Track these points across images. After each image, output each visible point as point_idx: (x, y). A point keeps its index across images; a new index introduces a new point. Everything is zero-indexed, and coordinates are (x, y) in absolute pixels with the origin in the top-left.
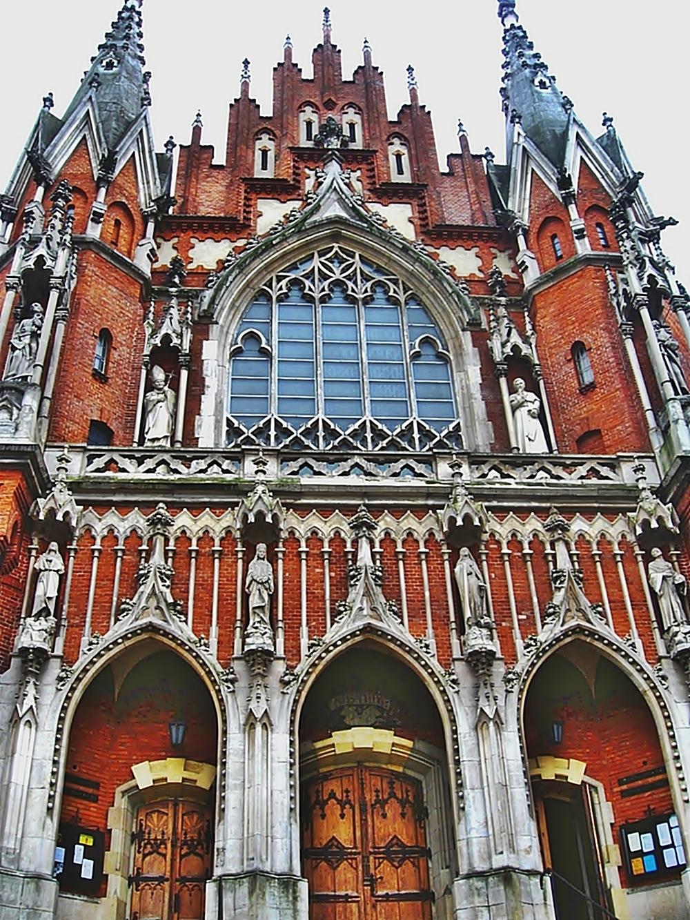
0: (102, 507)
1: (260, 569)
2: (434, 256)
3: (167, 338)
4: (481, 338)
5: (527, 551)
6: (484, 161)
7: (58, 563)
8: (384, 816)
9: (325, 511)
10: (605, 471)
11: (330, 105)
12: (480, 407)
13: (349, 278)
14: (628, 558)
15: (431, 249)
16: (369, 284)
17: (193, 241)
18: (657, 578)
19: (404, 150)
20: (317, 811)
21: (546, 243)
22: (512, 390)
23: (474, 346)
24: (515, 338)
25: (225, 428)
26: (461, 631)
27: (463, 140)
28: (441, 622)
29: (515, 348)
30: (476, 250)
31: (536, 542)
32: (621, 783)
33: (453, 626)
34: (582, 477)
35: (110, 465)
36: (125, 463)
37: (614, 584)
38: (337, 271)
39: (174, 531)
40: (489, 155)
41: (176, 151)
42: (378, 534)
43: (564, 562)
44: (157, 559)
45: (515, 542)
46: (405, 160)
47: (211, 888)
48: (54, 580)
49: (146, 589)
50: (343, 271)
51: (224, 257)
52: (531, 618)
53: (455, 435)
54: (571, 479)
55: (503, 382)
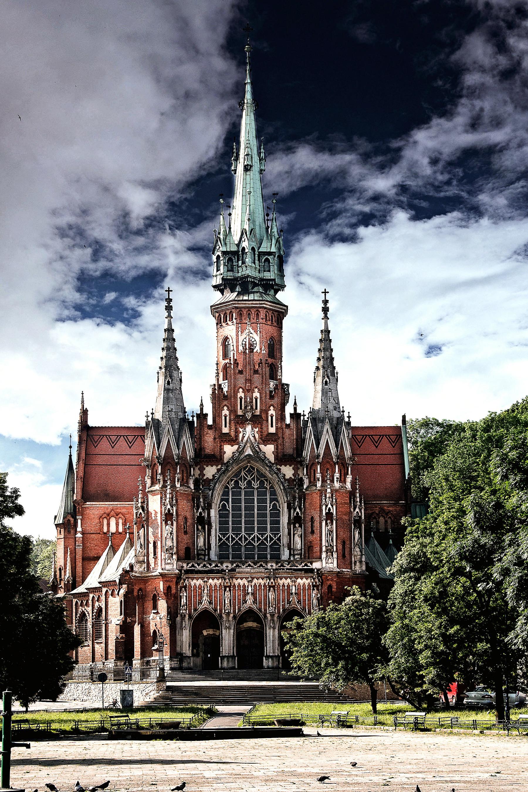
0: (193, 579)
1: (227, 594)
2: (279, 470)
3: (201, 513)
4: (289, 508)
5: (286, 588)
6: (302, 418)
7: (185, 594)
9: (242, 579)
10: (309, 564)
11: (248, 391)
12: (286, 530)
13: (253, 479)
14: (309, 589)
15: (279, 467)
16: (258, 482)
17: (205, 466)
18: (314, 595)
21: (312, 471)
22: (295, 527)
24: (298, 510)
25: (218, 538)
26: (269, 607)
27: (295, 409)
28: (265, 605)
29: (298, 513)
30: (293, 466)
31: (288, 586)
35: (193, 566)
36: (196, 565)
37: (304, 595)
39: (208, 584)
40: (304, 415)
41: (195, 419)
42: (253, 584)
43: (294, 591)
44: (206, 591)
45: (284, 585)
46: (274, 418)
48: (185, 597)
49: (204, 599)
52: (285, 604)
53: (279, 539)
54: (300, 567)
55: (292, 526)
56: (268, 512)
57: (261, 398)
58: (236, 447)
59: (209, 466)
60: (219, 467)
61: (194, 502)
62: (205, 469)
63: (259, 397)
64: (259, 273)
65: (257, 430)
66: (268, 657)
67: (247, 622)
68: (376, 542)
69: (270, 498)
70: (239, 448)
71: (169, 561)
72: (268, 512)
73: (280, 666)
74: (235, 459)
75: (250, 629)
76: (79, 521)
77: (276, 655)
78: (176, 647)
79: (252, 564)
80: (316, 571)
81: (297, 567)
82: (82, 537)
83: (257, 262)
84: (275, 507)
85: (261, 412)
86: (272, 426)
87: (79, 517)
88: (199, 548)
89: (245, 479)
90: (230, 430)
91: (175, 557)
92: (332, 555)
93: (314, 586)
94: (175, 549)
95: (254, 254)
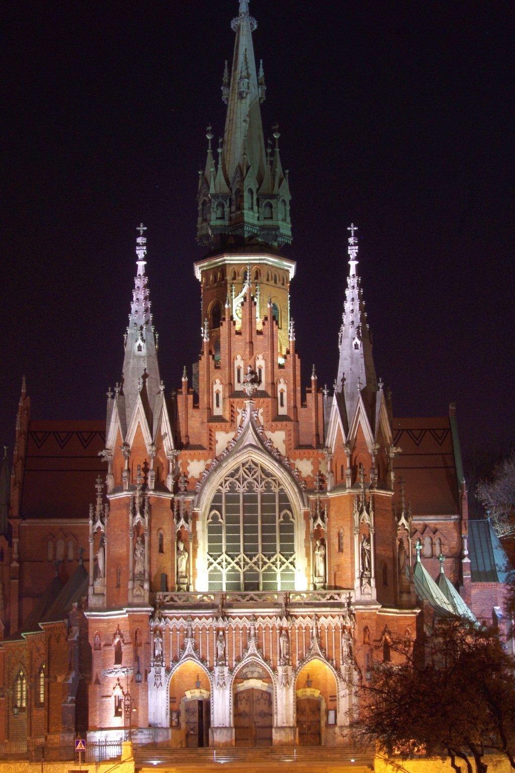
8: (259, 704)
16: (263, 483)
18: (343, 640)
19: (285, 389)
20: (239, 703)
23: (305, 518)
24: (319, 521)
29: (319, 526)
32: (330, 697)
33: (278, 655)
34: (328, 600)
38: (250, 475)
46: (285, 395)
47: (210, 731)
50: (253, 475)
51: (202, 471)
54: (324, 601)
56: (277, 524)
57: (267, 367)
58: (232, 435)
59: (195, 461)
60: (209, 461)
61: (173, 511)
62: (189, 464)
63: (264, 366)
64: (258, 219)
65: (261, 411)
66: (277, 728)
67: (248, 679)
68: (423, 568)
69: (280, 506)
70: (236, 435)
71: (138, 593)
72: (277, 524)
73: (297, 741)
74: (230, 452)
75: (252, 690)
76: (15, 546)
77: (291, 725)
78: (147, 715)
79: (256, 598)
80: (346, 604)
81: (319, 600)
82: (20, 567)
83: (255, 208)
84: (286, 517)
85: (266, 387)
86: (282, 405)
87: (15, 540)
88: (180, 574)
89: (245, 479)
90: (224, 410)
91: (146, 586)
92: (369, 583)
93: (344, 627)
94: (147, 575)
95: (252, 198)
